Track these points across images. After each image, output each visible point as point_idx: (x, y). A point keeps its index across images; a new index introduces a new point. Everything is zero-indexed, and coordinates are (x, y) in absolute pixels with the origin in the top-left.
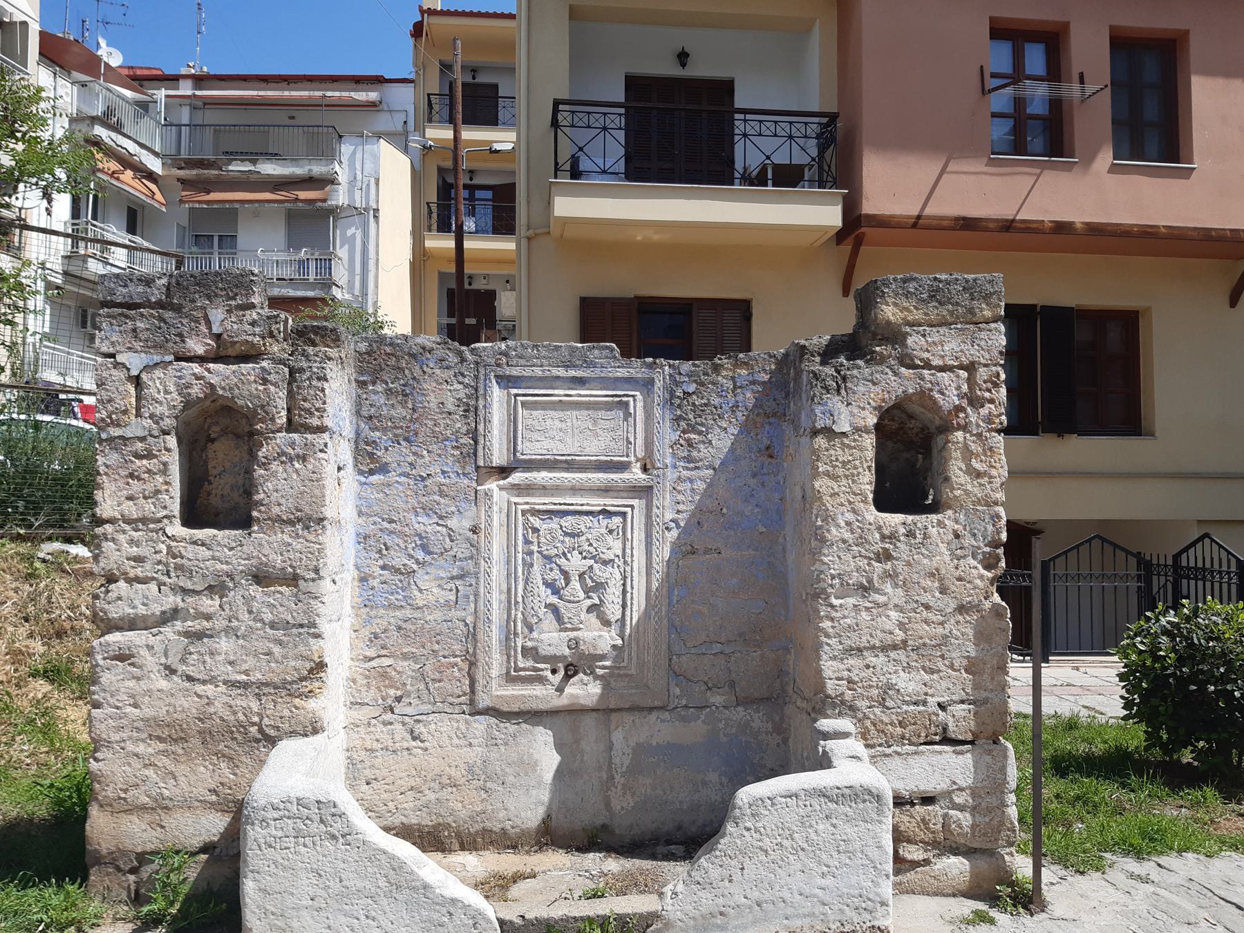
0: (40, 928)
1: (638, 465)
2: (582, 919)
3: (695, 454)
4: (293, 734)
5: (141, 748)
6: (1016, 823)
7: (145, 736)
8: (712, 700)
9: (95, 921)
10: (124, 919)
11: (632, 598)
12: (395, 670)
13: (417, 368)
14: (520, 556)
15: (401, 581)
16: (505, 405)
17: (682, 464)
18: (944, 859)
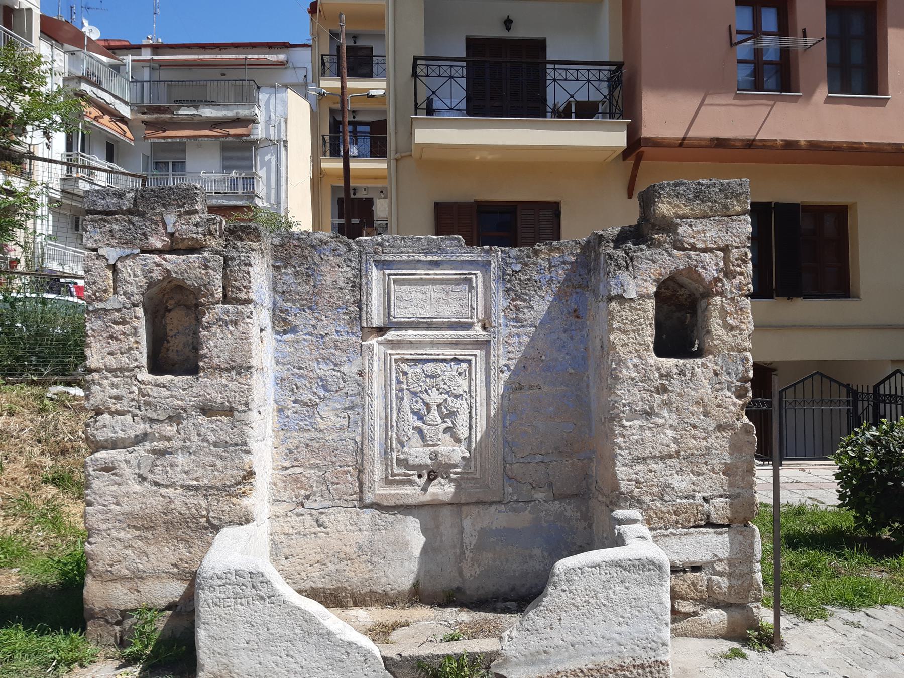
0: (54, 664)
1: (480, 324)
2: (443, 656)
3: (521, 316)
4: (231, 523)
5: (122, 535)
6: (761, 584)
7: (124, 525)
8: (536, 496)
9: (92, 659)
10: (113, 658)
11: (476, 422)
12: (305, 476)
13: (317, 255)
14: (394, 392)
15: (308, 411)
16: (381, 282)
17: (512, 323)
18: (708, 611)
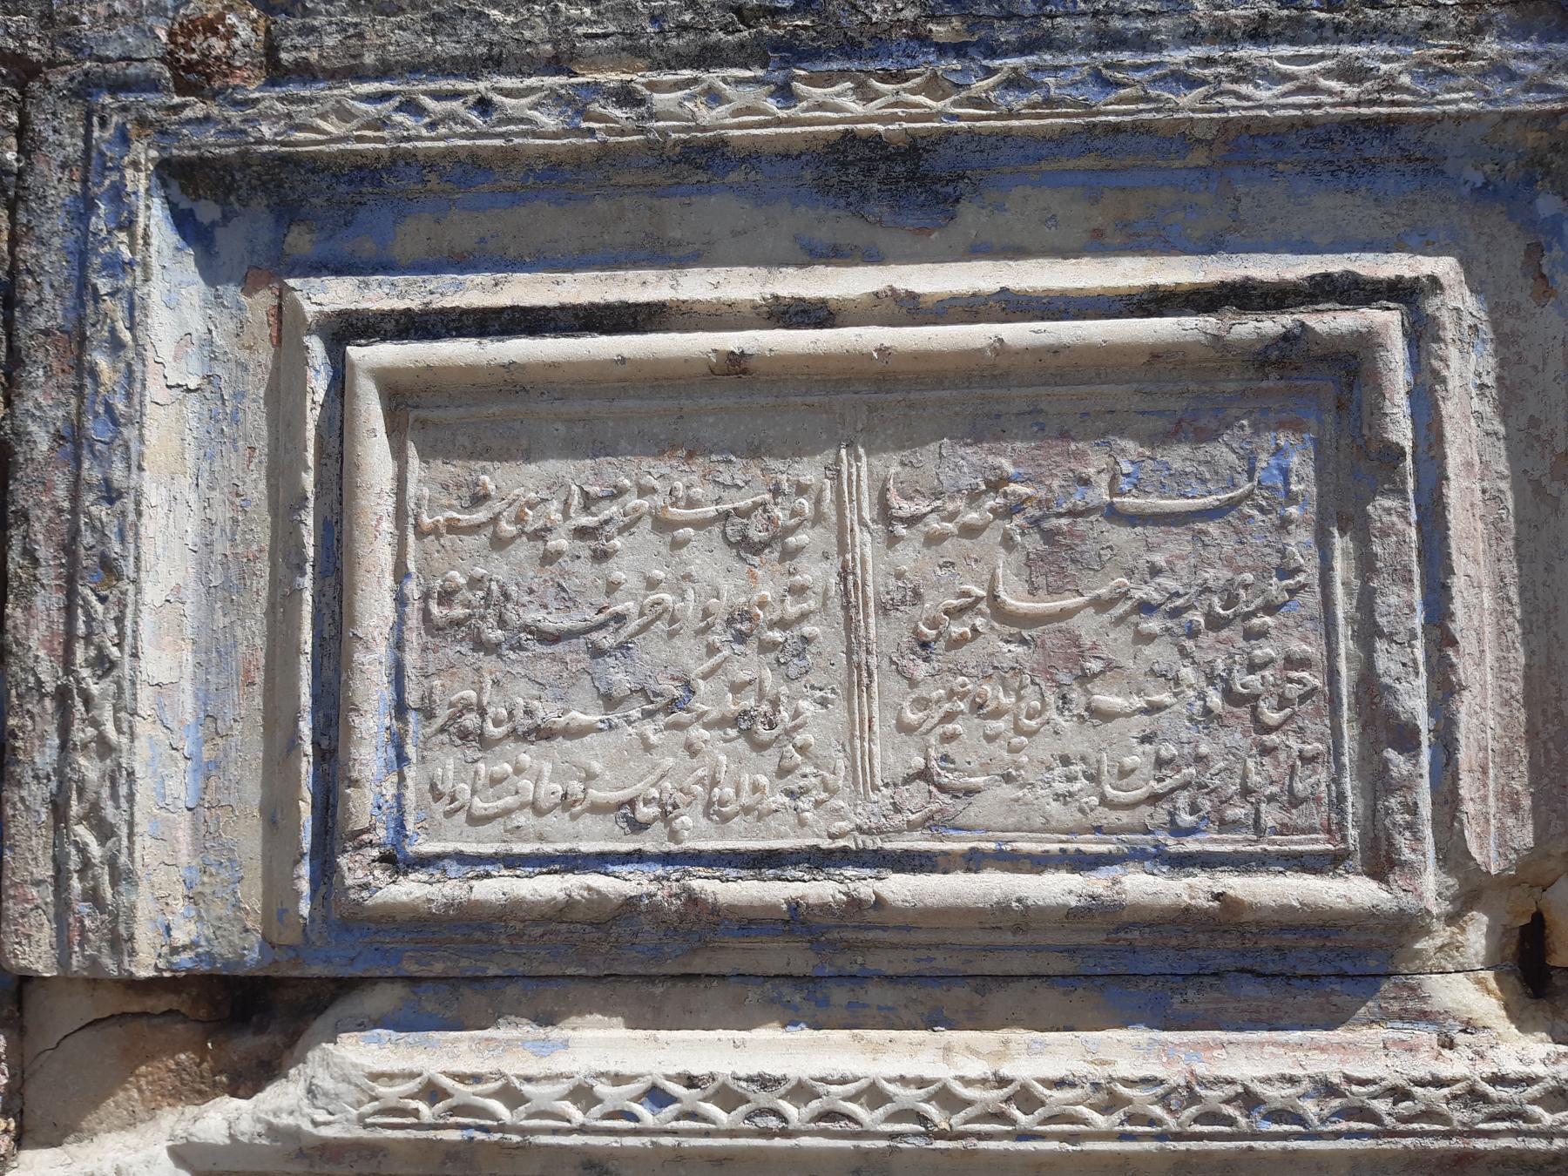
1: (1476, 936)
16: (256, 419)
